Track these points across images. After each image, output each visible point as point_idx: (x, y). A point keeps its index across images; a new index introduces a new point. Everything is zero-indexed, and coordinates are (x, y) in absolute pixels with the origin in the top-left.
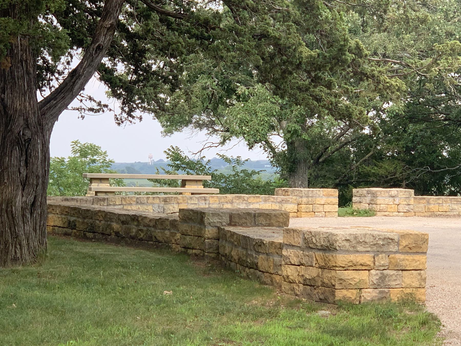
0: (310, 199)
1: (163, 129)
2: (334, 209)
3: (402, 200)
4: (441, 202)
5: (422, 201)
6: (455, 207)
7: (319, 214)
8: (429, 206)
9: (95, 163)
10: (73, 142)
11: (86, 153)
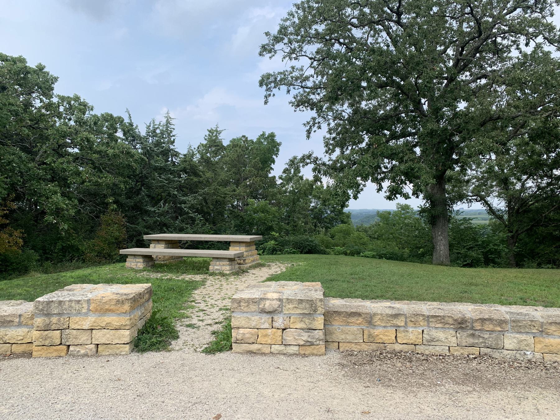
0: (54, 319)
2: (119, 338)
3: (292, 320)
4: (403, 324)
5: (353, 320)
6: (441, 335)
7: (77, 349)
8: (372, 331)
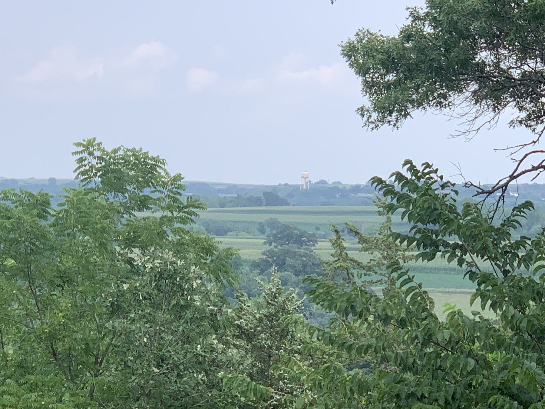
1: (366, 101)
9: (148, 208)
10: (79, 144)
11: (119, 179)
